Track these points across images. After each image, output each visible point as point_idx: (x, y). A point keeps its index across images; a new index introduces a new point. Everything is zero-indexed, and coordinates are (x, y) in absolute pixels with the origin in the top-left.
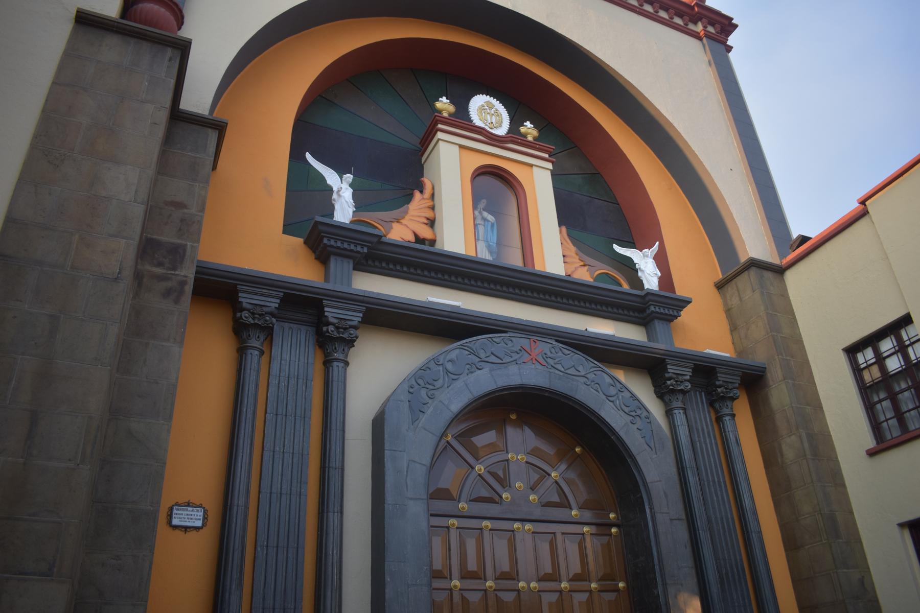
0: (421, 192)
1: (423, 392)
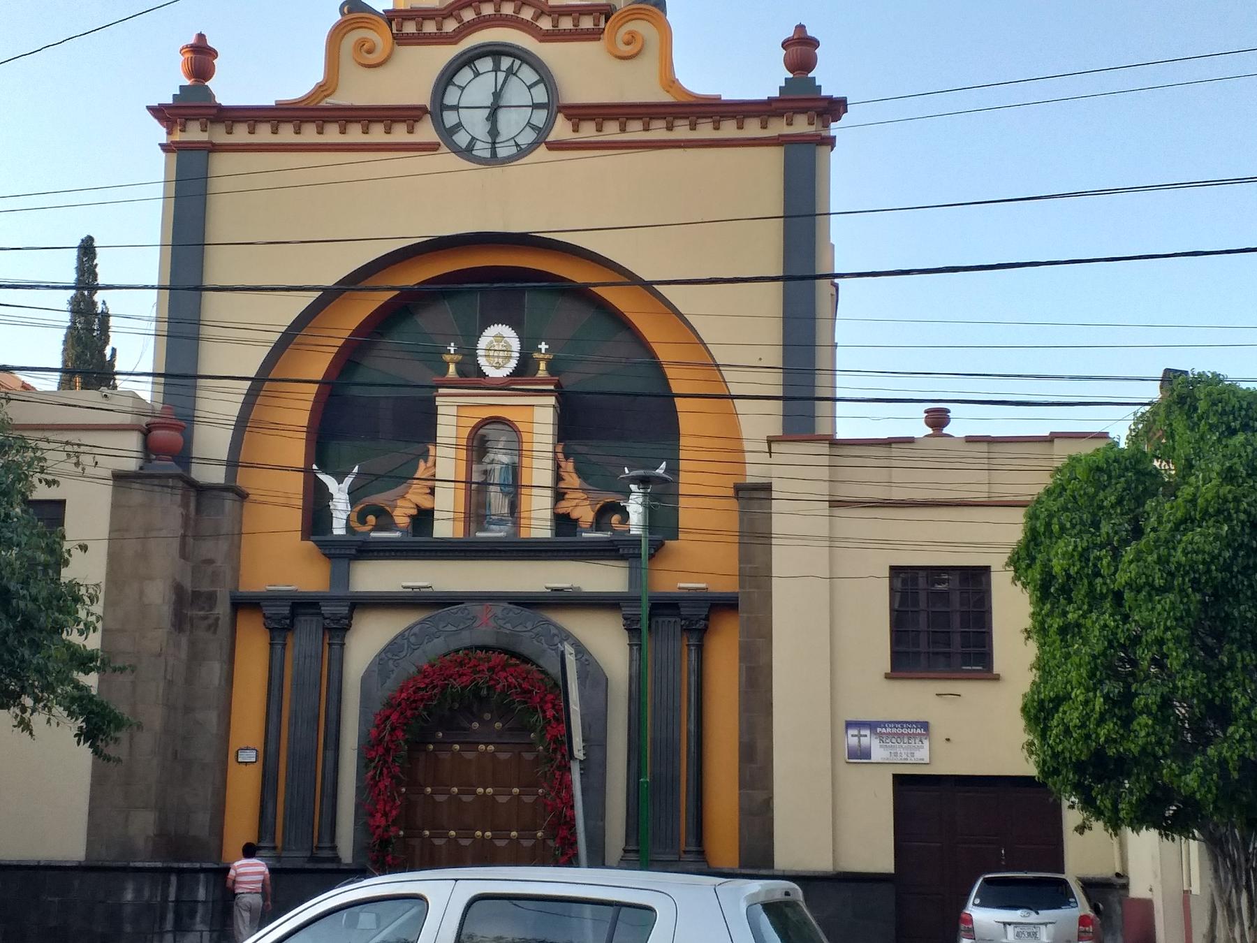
0: (426, 462)
1: (391, 662)
